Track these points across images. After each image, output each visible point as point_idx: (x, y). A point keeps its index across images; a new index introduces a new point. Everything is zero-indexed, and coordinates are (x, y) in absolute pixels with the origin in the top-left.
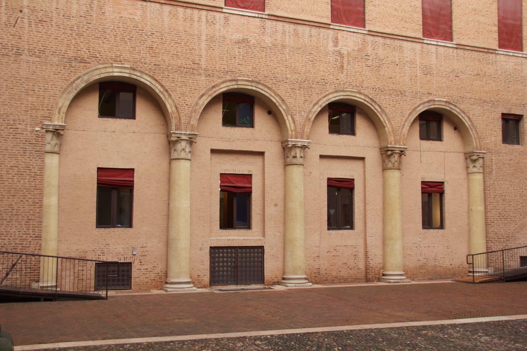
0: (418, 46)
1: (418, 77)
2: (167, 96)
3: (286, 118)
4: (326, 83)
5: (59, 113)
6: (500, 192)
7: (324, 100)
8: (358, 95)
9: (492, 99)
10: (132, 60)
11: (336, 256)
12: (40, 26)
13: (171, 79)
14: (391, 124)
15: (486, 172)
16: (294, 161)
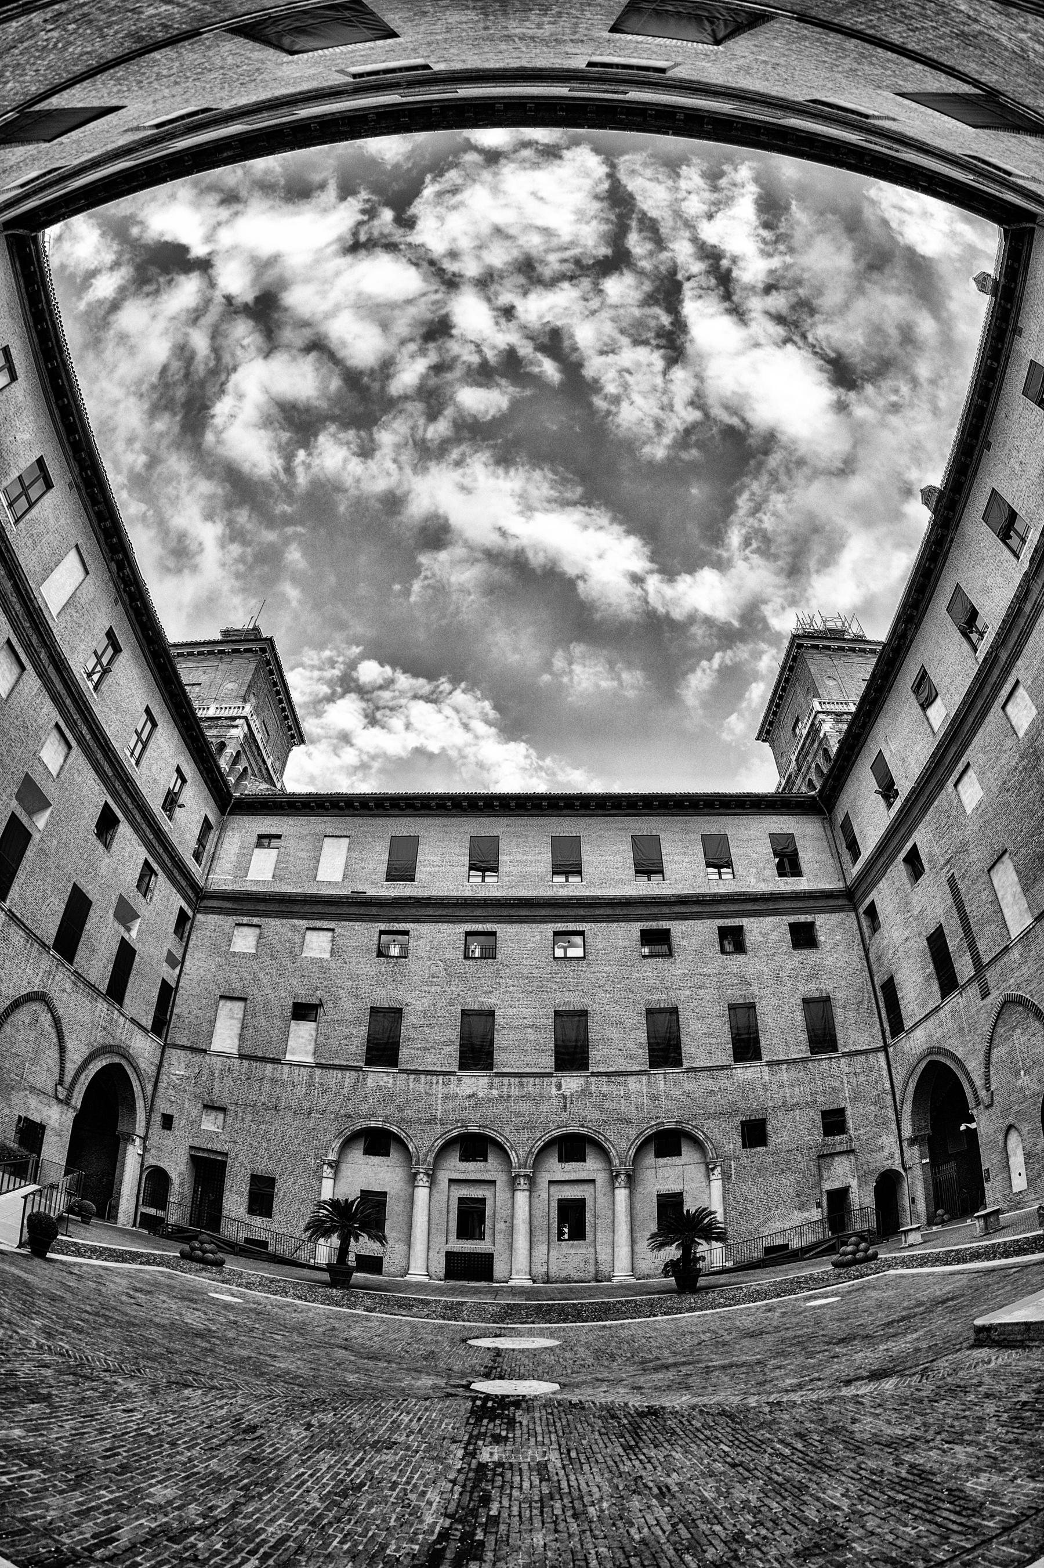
0: (644, 1078)
15: (726, 1177)
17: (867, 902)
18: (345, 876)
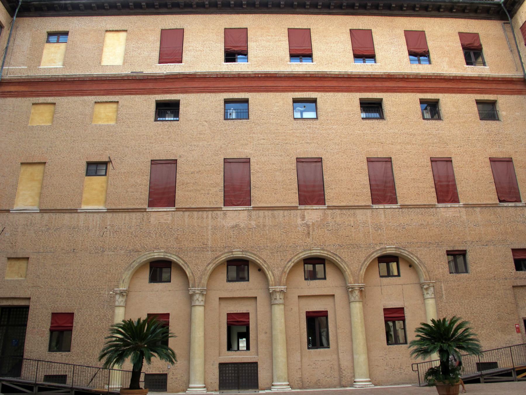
0: (369, 212)
1: (371, 233)
2: (186, 267)
3: (267, 273)
4: (296, 246)
5: (123, 283)
6: (451, 312)
7: (296, 258)
8: (322, 252)
9: (436, 241)
10: (165, 247)
11: (315, 368)
12: (115, 234)
13: (189, 256)
14: (350, 269)
15: (438, 297)
16: (276, 302)
18: (124, 63)
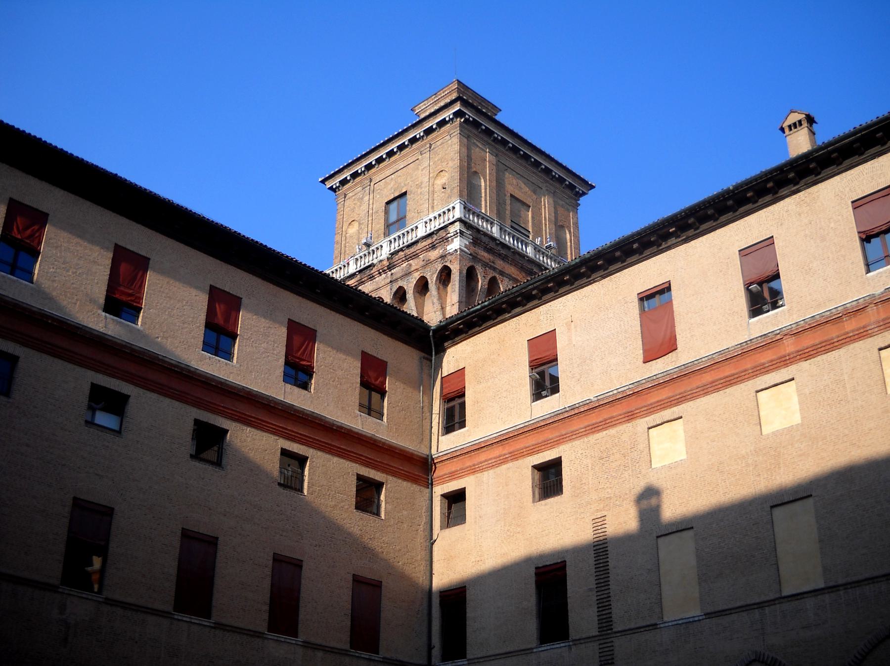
17: (453, 486)
